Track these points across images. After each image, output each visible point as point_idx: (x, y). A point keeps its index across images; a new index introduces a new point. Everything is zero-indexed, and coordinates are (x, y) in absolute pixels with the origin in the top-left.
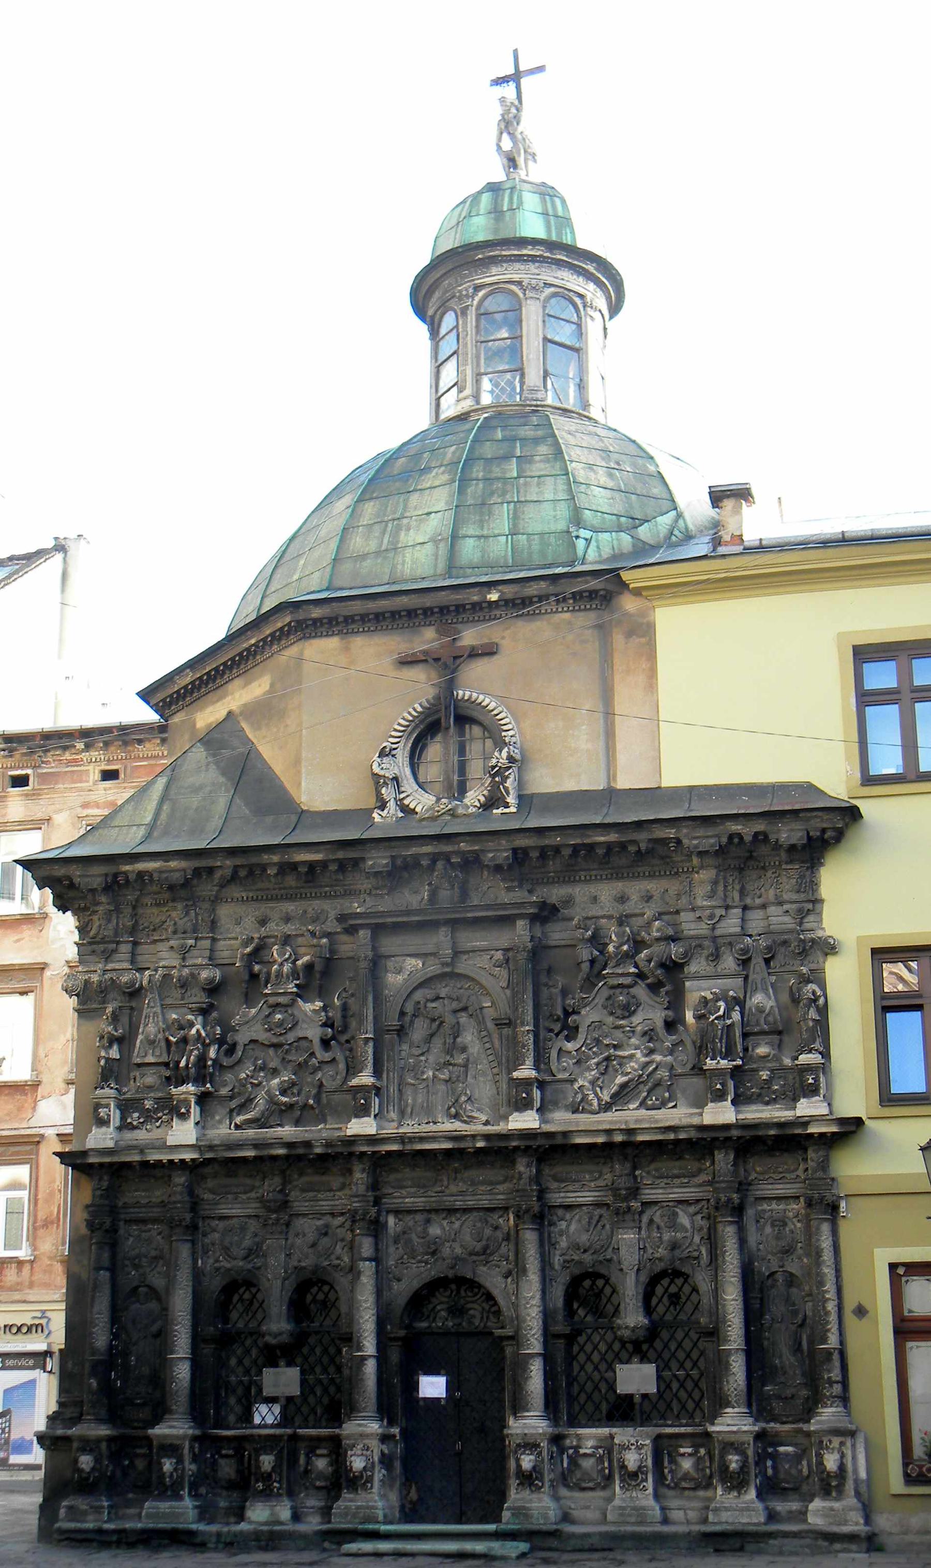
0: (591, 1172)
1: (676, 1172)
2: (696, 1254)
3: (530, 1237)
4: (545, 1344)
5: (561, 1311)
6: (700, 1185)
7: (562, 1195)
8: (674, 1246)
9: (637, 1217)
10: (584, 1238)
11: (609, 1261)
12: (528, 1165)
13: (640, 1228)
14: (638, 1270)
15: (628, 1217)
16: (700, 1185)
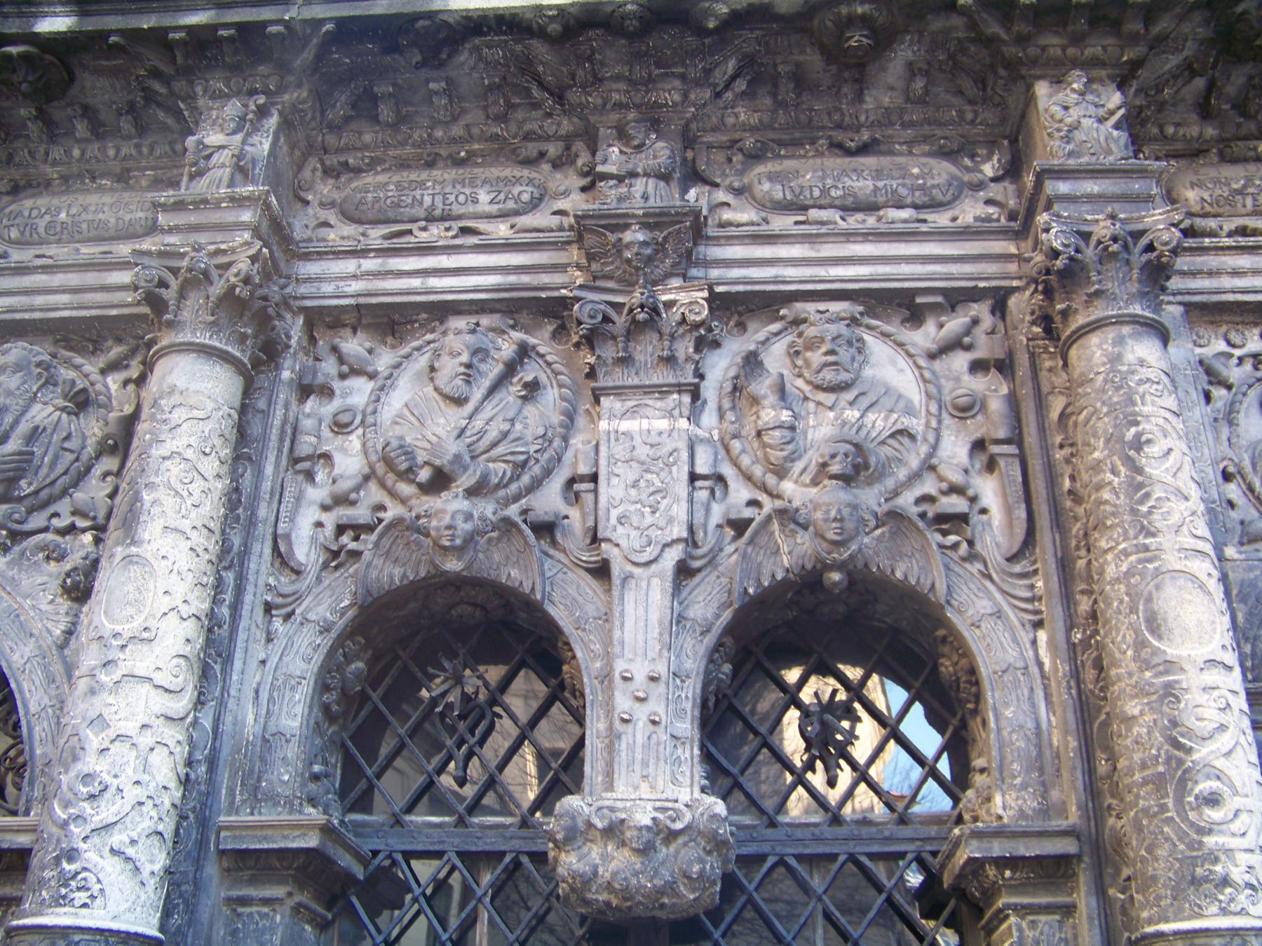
0: (498, 185)
1: (863, 186)
2: (955, 504)
3: (192, 395)
4: (179, 891)
5: (292, 751)
6: (965, 233)
7: (370, 264)
8: (857, 466)
9: (685, 348)
10: (438, 432)
11: (546, 529)
12: (246, 125)
13: (696, 394)
14: (684, 571)
15: (646, 349)
16: (965, 233)
